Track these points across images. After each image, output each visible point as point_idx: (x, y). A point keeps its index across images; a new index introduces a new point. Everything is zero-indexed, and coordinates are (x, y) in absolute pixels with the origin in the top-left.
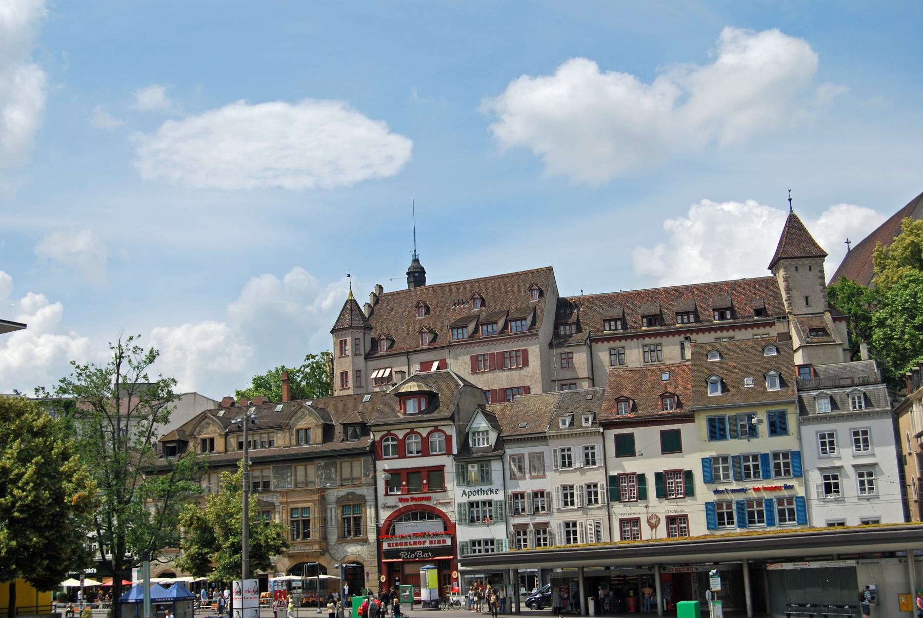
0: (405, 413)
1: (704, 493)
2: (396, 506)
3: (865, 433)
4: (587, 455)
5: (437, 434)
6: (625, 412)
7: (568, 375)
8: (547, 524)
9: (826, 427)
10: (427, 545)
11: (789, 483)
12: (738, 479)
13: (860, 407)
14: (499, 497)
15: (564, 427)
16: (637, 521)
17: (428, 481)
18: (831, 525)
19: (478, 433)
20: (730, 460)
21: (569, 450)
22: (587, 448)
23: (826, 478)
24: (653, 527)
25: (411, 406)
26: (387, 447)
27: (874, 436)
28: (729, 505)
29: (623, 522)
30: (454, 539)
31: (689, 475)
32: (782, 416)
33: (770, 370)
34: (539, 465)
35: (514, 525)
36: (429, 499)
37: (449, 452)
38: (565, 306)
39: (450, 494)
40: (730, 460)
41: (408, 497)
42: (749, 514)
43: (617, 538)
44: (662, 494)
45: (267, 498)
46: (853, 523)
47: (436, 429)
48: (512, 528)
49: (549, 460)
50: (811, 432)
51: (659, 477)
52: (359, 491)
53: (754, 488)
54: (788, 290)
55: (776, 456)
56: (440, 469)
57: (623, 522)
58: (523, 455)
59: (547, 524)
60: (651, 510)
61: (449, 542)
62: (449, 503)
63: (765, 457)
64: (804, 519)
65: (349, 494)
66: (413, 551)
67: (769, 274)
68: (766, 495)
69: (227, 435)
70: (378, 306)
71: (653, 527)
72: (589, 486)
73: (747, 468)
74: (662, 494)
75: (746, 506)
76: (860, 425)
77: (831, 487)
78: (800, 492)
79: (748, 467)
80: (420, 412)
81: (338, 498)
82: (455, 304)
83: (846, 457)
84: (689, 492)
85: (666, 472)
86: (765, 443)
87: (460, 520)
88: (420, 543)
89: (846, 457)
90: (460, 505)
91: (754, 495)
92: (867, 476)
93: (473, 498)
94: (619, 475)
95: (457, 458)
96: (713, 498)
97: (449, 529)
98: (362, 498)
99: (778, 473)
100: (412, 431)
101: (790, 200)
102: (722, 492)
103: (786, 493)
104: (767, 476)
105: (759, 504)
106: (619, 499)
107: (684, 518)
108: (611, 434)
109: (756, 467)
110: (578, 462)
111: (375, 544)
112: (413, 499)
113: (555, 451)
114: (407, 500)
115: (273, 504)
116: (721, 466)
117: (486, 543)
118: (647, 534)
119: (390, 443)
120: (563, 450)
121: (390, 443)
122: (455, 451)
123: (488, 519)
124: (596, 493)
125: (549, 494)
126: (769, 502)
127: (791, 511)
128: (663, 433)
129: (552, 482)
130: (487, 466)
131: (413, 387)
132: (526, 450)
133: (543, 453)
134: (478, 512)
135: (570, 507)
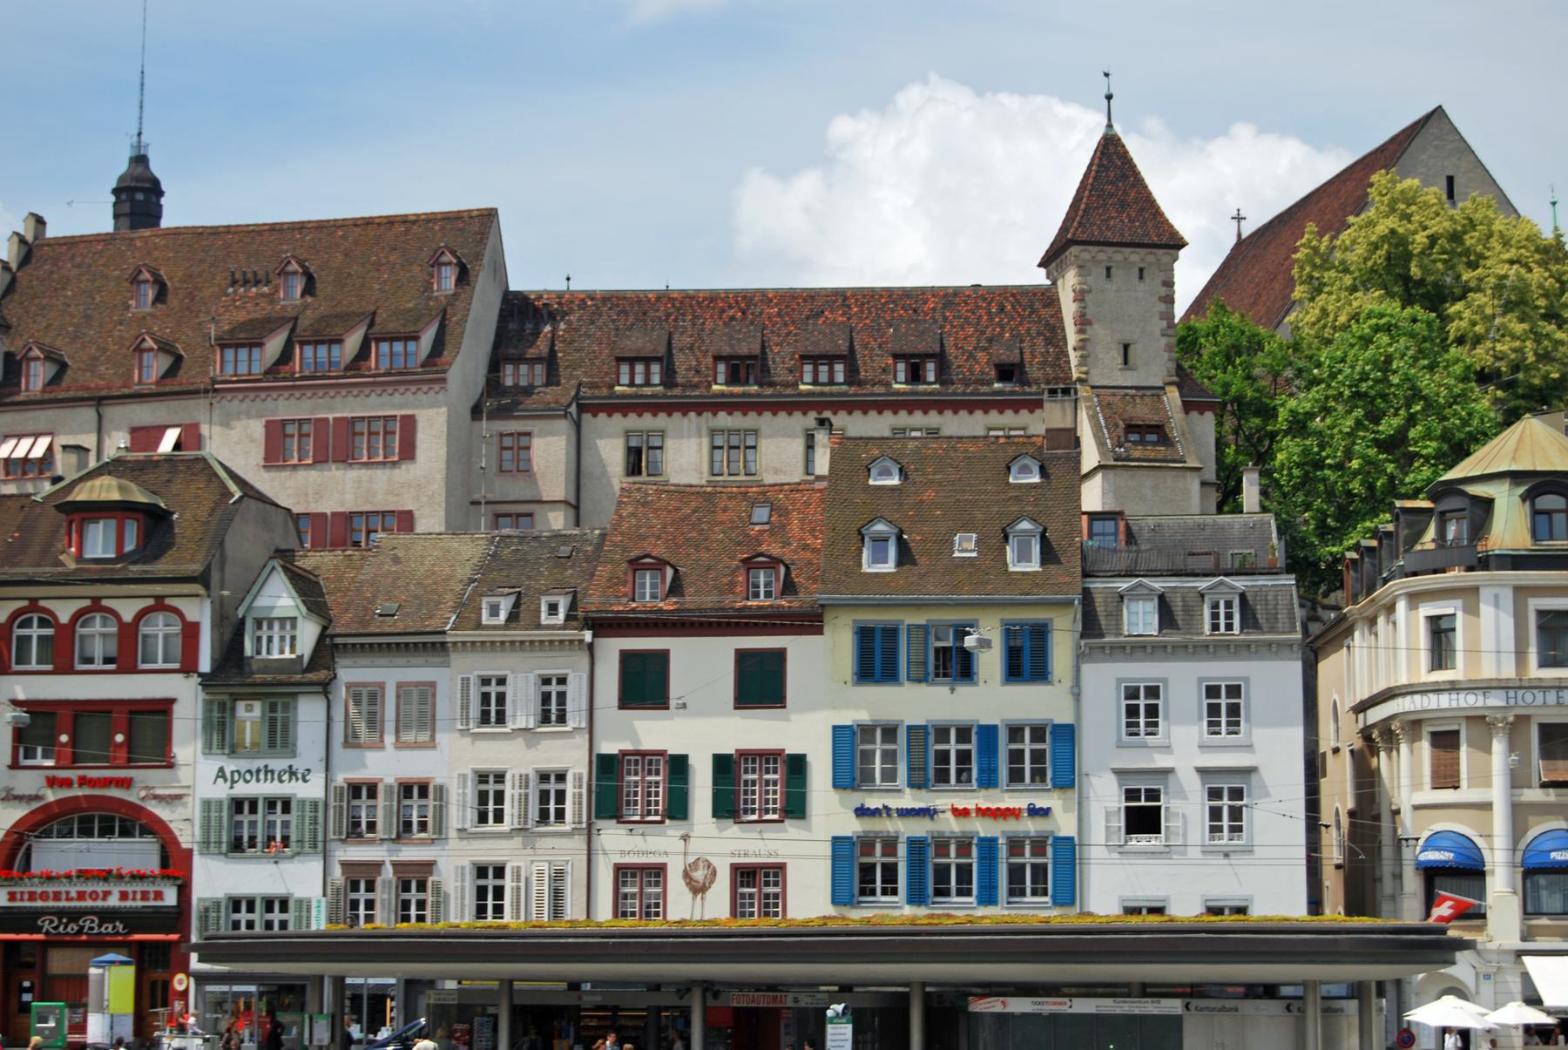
0: (79, 557)
1: (833, 815)
2: (37, 798)
3: (1234, 691)
4: (546, 698)
5: (160, 618)
6: (650, 594)
7: (514, 489)
8: (429, 866)
9: (1143, 671)
10: (114, 901)
11: (1041, 802)
12: (916, 784)
13: (1229, 627)
14: (313, 789)
15: (494, 621)
16: (657, 872)
17: (129, 739)
18: (1132, 911)
19: (271, 621)
20: (902, 736)
21: (502, 681)
22: (546, 681)
23: (1132, 794)
24: (698, 889)
25: (99, 542)
26: (24, 641)
27: (1253, 701)
28: (890, 845)
29: (622, 872)
30: (184, 891)
31: (797, 765)
32: (1041, 633)
33: (1017, 520)
34: (422, 713)
35: (346, 865)
36: (126, 783)
37: (188, 666)
38: (522, 315)
39: (183, 775)
40: (902, 736)
41: (73, 774)
42: (935, 870)
43: (604, 912)
44: (727, 807)
46: (1186, 908)
47: (160, 605)
48: (337, 873)
49: (447, 704)
50: (1104, 682)
51: (723, 765)
53: (956, 810)
54: (1083, 322)
55: (1015, 732)
56: (162, 709)
57: (622, 872)
58: (382, 686)
59: (429, 866)
60: (697, 847)
61: (171, 898)
62: (179, 797)
63: (988, 733)
64: (1068, 895)
66: (74, 915)
67: (1039, 278)
68: (983, 828)
70: (29, 269)
71: (698, 889)
72: (544, 777)
73: (943, 757)
74: (727, 807)
75: (931, 851)
76: (1223, 670)
77: (1143, 819)
78: (1065, 824)
79: (944, 756)
80: (121, 556)
82: (234, 283)
83: (1183, 747)
84: (795, 808)
85: (746, 755)
86: (990, 699)
87: (206, 843)
88: (94, 896)
89: (1183, 747)
90: (207, 804)
91: (951, 825)
92: (1229, 798)
93: (243, 790)
94: (624, 753)
95: (207, 681)
96: (852, 826)
97: (175, 863)
99: (1016, 776)
100: (96, 605)
101: (1109, 97)
102: (874, 813)
103: (1030, 826)
104: (988, 781)
105: (964, 847)
106: (618, 817)
107: (776, 872)
108: (612, 649)
109: (964, 757)
110: (522, 714)
112: (83, 781)
113: (465, 682)
114: (67, 783)
116: (878, 747)
117: (269, 905)
118: (680, 907)
119: (35, 632)
120: (486, 681)
121: (35, 632)
122: (205, 665)
123: (278, 845)
124: (561, 797)
125: (441, 790)
126: (989, 845)
127: (1039, 872)
128: (742, 656)
129: (452, 759)
130: (286, 707)
131: (106, 489)
132: (390, 675)
133: (433, 685)
134: (253, 824)
135: (491, 826)
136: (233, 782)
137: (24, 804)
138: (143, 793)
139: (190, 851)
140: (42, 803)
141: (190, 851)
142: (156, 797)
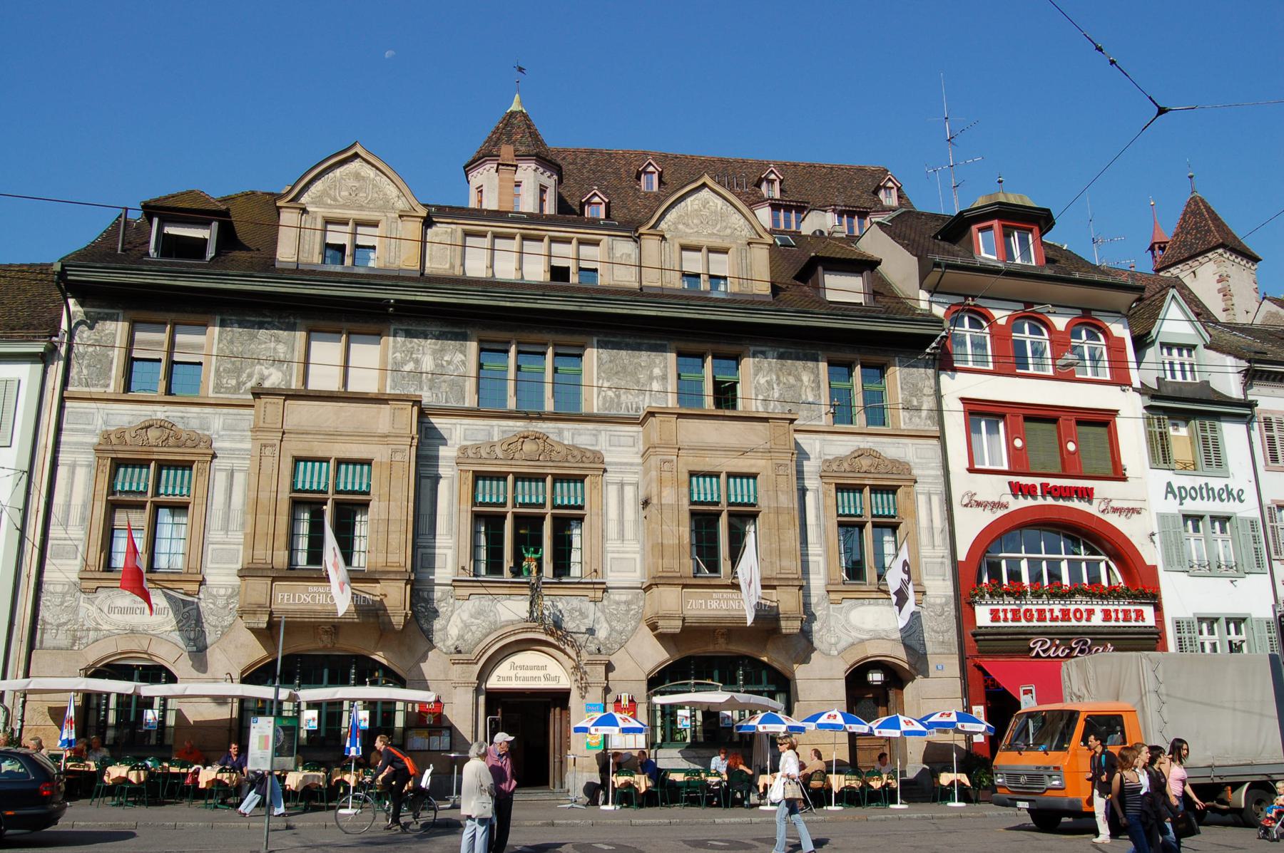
10: (1097, 620)
17: (1062, 447)
36: (1086, 494)
45: (568, 434)
52: (891, 449)
56: (1103, 420)
65: (860, 454)
69: (428, 223)
81: (828, 462)
90: (1162, 518)
93: (1192, 506)
98: (902, 468)
111: (951, 610)
112: (1047, 490)
115: (598, 457)
136: (1182, 499)
137: (988, 511)
138: (1103, 507)
139: (1154, 568)
140: (1006, 511)
141: (1154, 568)
142: (1115, 510)
